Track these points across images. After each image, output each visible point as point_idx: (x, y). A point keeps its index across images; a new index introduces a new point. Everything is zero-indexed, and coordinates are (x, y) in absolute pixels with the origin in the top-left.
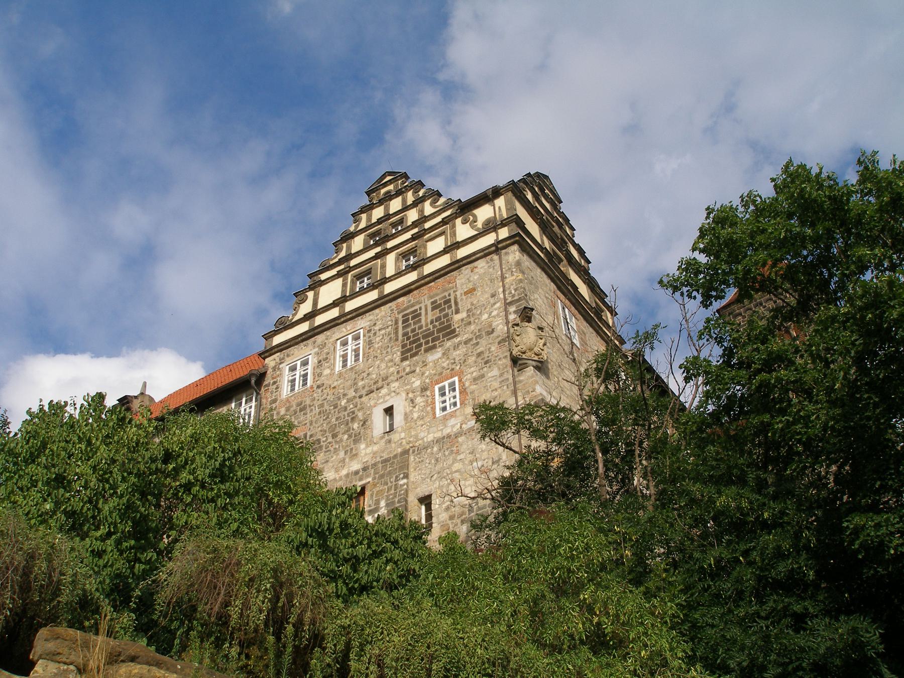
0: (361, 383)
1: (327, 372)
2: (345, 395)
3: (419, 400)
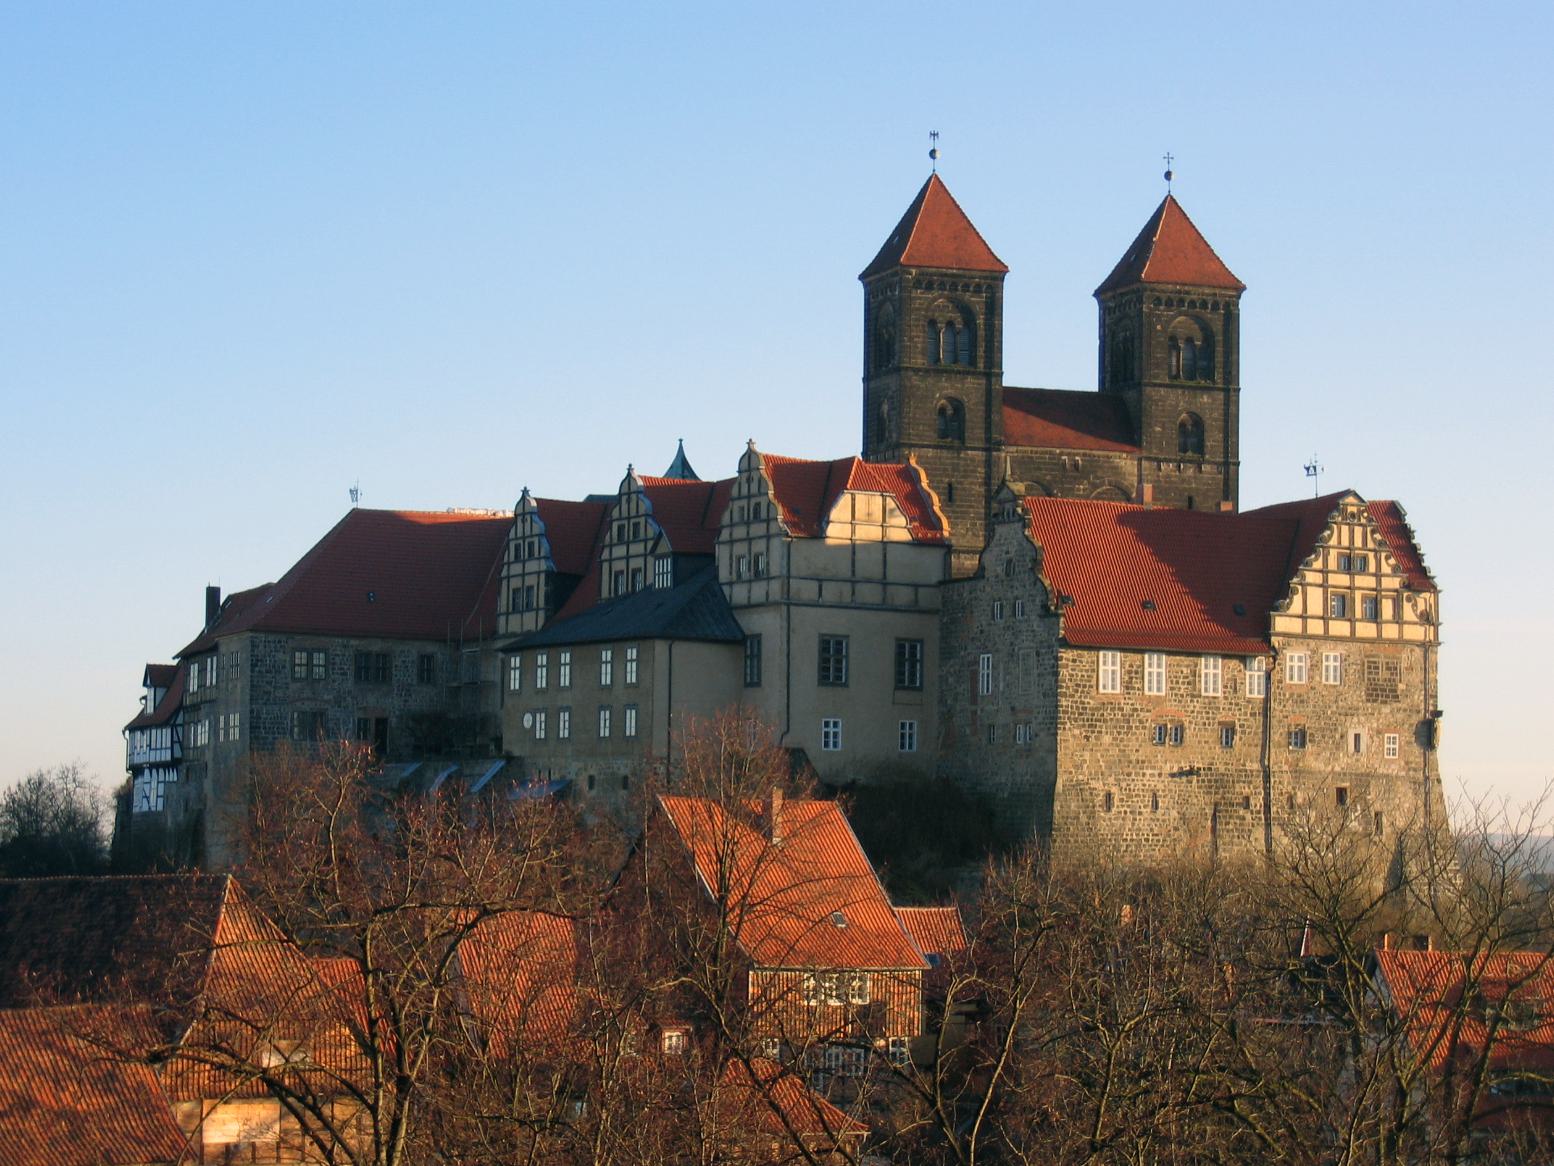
0: (1340, 703)
1: (1318, 678)
2: (1330, 707)
3: (1375, 738)
